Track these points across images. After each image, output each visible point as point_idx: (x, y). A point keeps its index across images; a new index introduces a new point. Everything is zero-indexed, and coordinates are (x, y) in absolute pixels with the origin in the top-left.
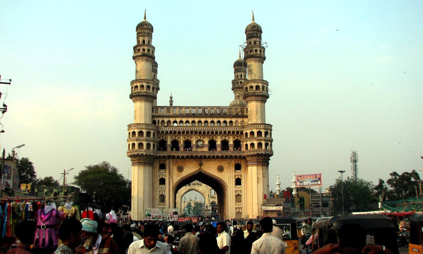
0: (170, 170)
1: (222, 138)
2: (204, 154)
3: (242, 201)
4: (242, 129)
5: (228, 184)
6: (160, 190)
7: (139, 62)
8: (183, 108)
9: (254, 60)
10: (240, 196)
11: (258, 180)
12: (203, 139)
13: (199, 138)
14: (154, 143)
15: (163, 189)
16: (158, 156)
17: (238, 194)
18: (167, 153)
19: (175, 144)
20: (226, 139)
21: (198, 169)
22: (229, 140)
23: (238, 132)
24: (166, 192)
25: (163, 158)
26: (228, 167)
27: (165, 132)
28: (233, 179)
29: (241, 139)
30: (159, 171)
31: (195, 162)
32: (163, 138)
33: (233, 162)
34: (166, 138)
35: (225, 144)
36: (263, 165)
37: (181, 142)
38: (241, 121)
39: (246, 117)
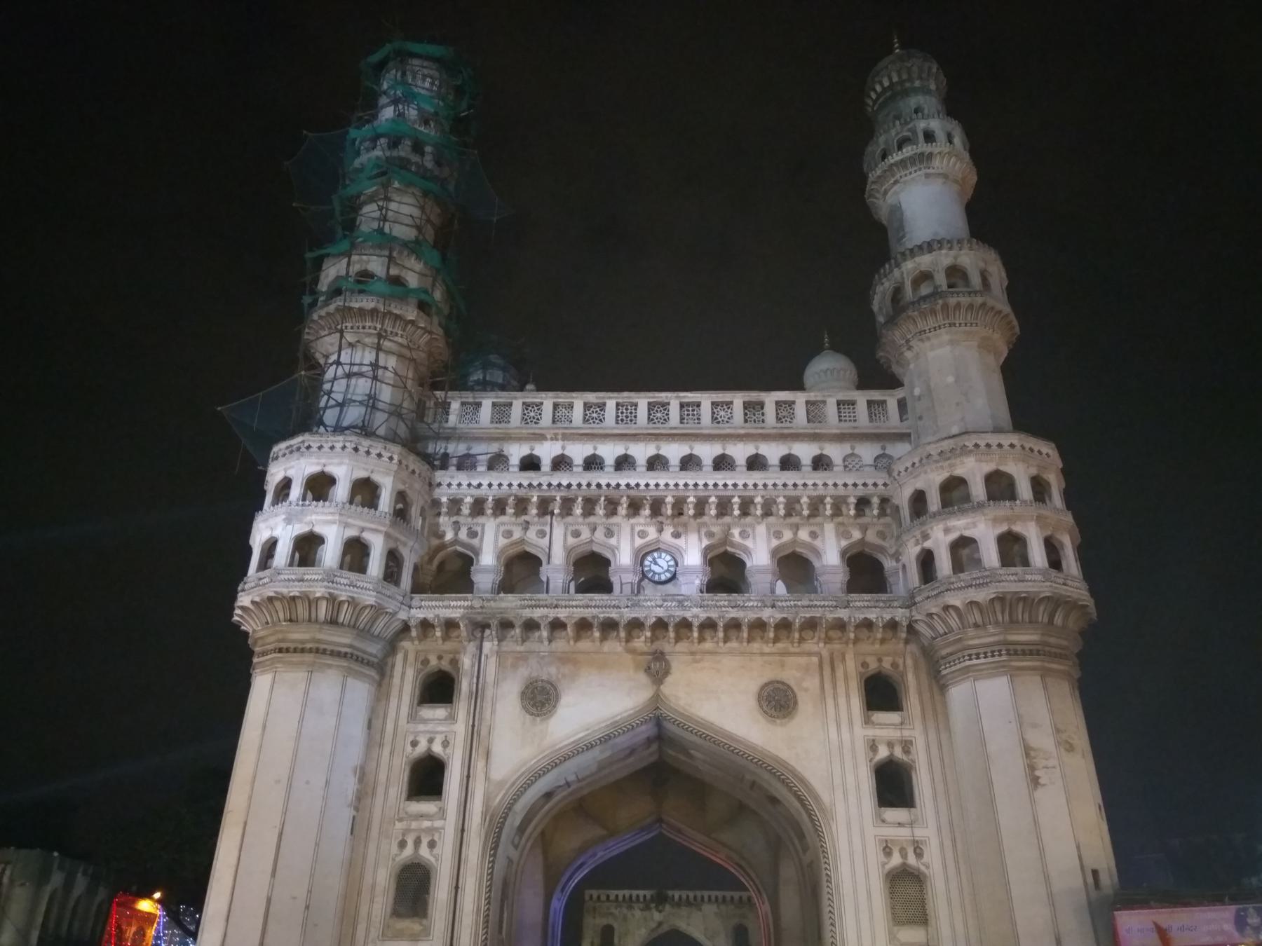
0: (481, 713)
1: (778, 535)
2: (679, 613)
3: (932, 921)
4: (885, 485)
5: (825, 797)
6: (406, 832)
10: (918, 876)
11: (1032, 768)
12: (677, 542)
14: (392, 545)
15: (426, 824)
16: (412, 623)
17: (904, 864)
18: (466, 604)
19: (522, 568)
20: (804, 544)
22: (817, 543)
23: (863, 503)
24: (439, 844)
25: (446, 637)
28: (856, 766)
29: (884, 544)
32: (456, 534)
33: (851, 665)
34: (472, 534)
35: (795, 567)
36: (1045, 673)
38: (877, 458)
39: (903, 437)
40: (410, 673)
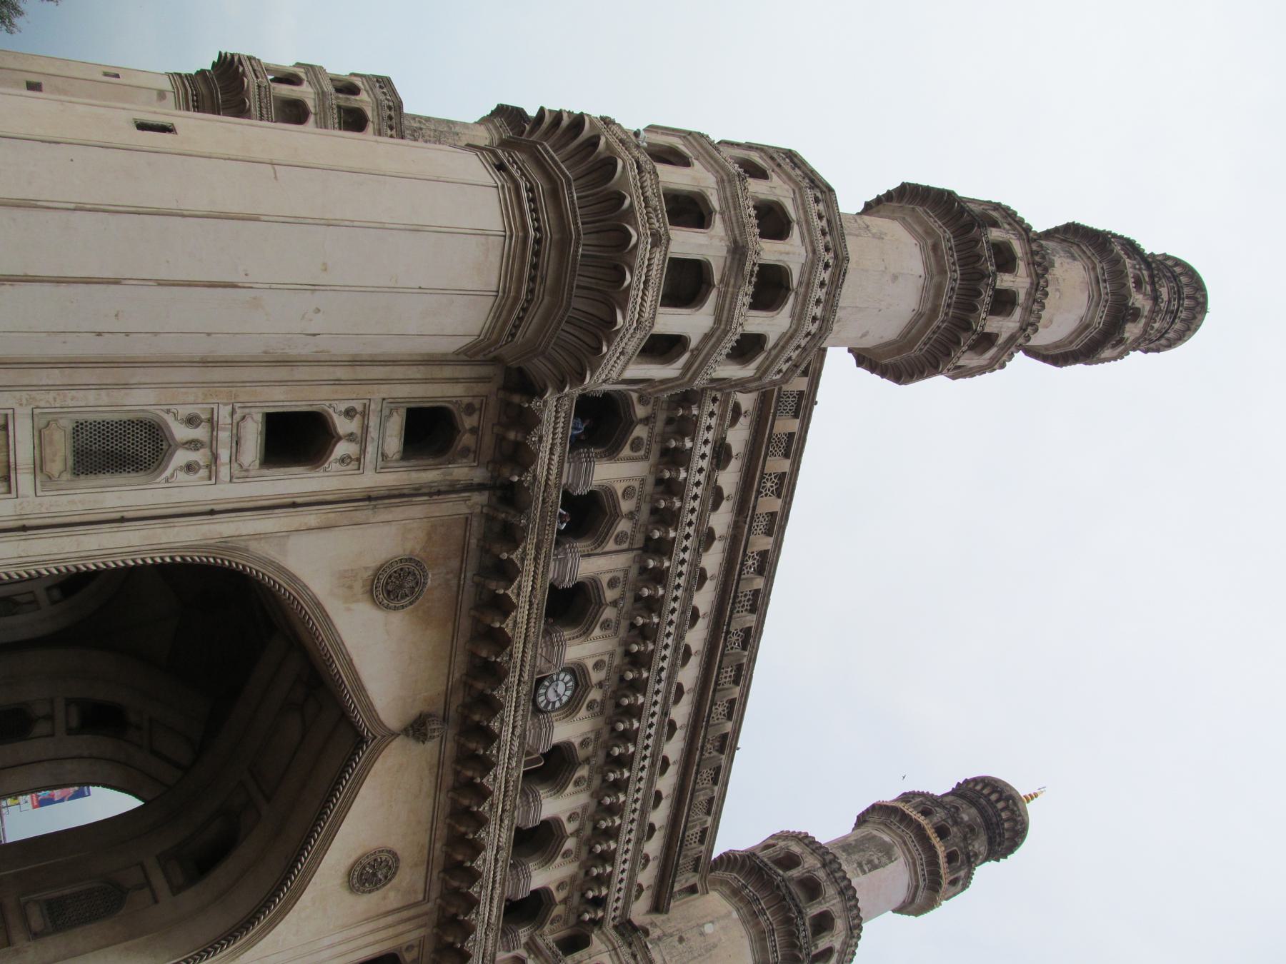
7: (1087, 276)
8: (771, 540)
9: (921, 884)
13: (595, 677)
15: (224, 455)
18: (552, 477)
21: (383, 716)
22: (559, 860)
26: (383, 909)
27: (688, 444)
30: (394, 403)
31: (440, 688)
33: (414, 936)
34: (636, 445)
37: (593, 559)
39: (659, 906)
40: (456, 391)
